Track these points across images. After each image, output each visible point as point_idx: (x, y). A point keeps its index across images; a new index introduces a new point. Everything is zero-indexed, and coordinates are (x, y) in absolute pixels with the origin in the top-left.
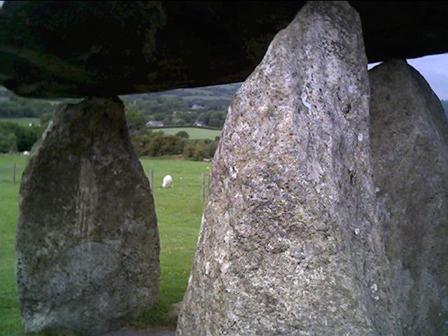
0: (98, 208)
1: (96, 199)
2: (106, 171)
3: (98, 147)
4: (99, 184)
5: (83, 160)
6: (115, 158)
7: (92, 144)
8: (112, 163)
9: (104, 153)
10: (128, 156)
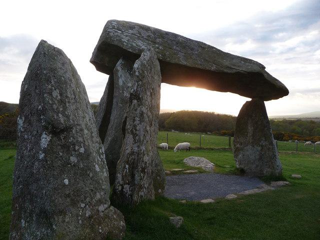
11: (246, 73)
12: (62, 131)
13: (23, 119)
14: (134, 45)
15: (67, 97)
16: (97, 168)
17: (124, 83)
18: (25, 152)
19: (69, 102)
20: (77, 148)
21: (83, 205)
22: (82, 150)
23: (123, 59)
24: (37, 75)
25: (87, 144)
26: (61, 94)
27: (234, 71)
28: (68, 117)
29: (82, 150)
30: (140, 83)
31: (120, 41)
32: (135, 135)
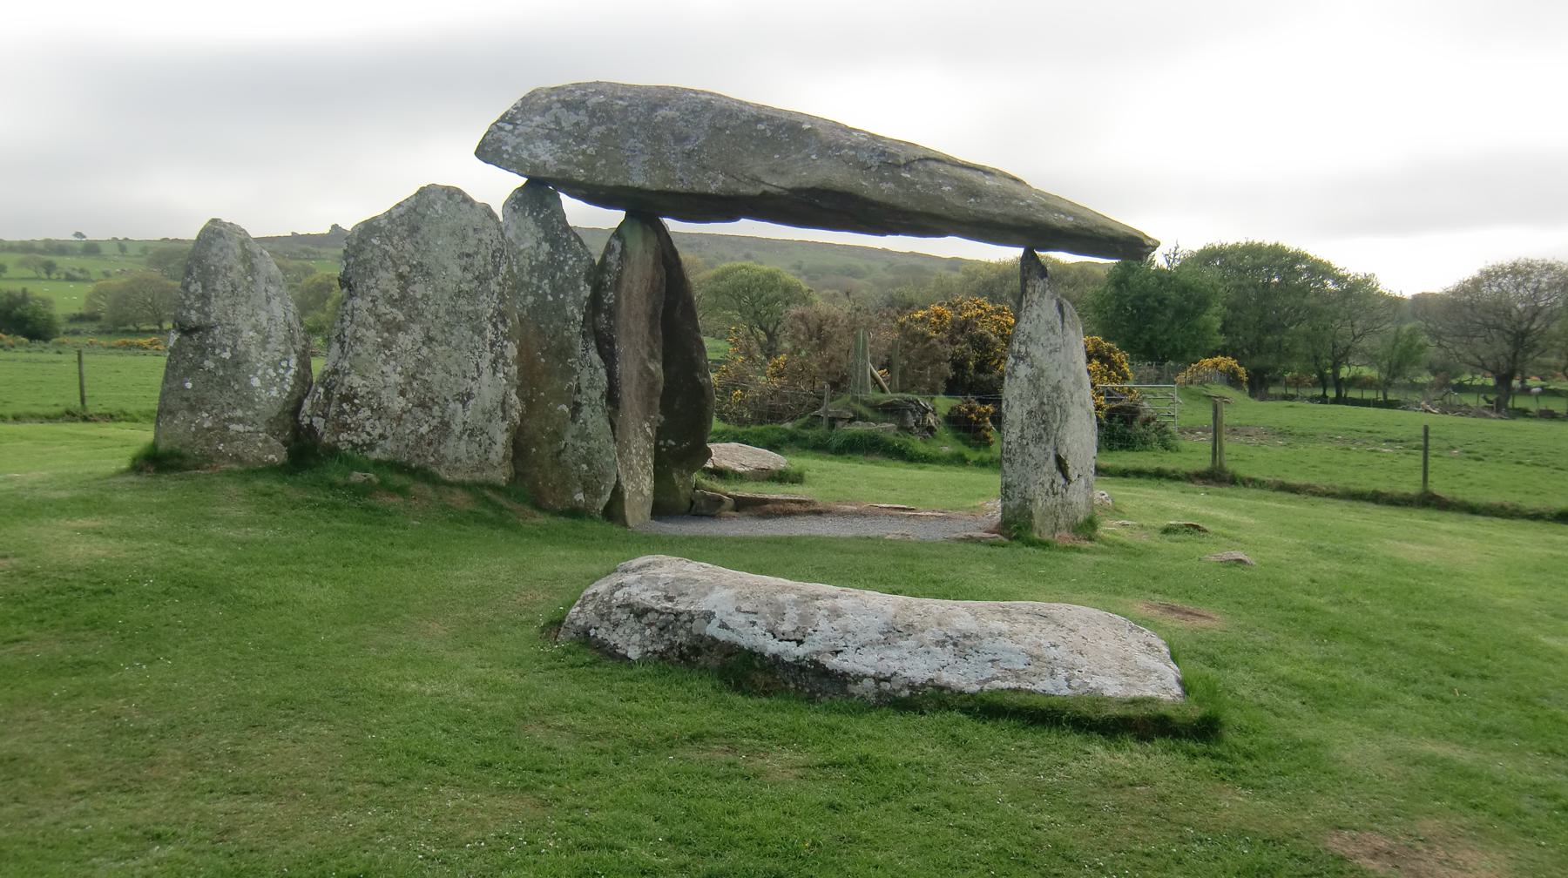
11: (786, 193)
12: (196, 329)
14: (525, 155)
15: (214, 290)
16: (256, 382)
19: (216, 296)
20: (217, 351)
21: (205, 415)
22: (227, 355)
25: (241, 348)
26: (204, 287)
28: (207, 315)
29: (227, 355)
30: (352, 260)
32: (342, 344)
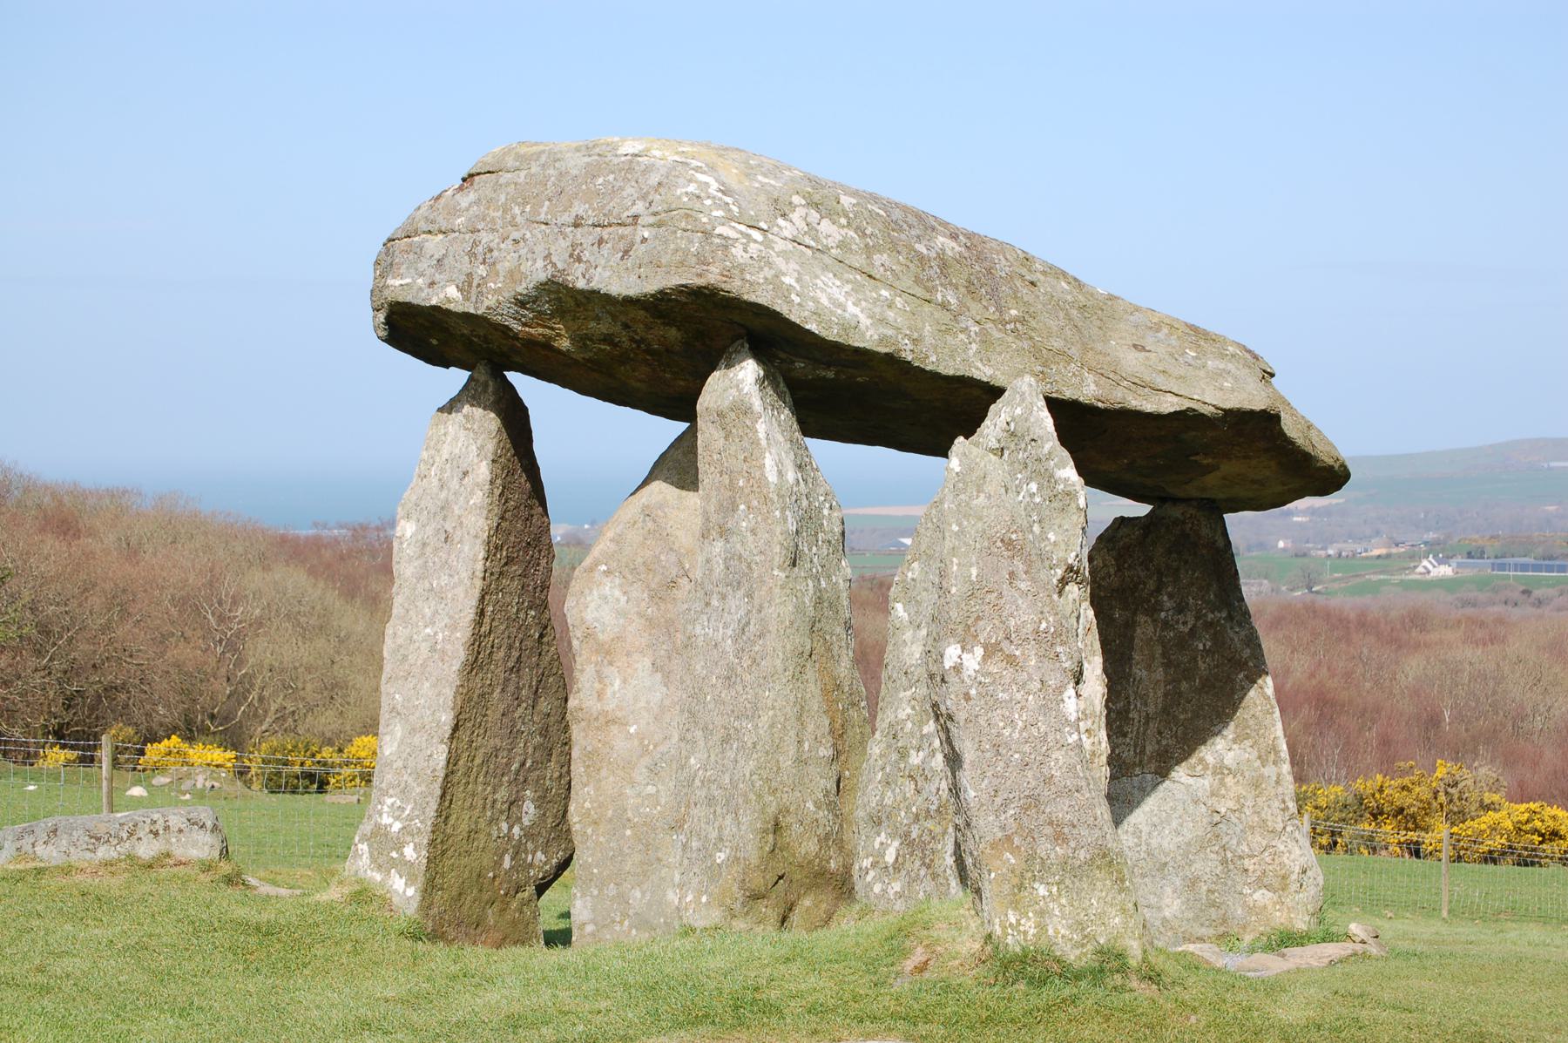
0: (1165, 710)
1: (1160, 694)
2: (1183, 643)
3: (1171, 596)
4: (1168, 665)
5: (1141, 618)
6: (1197, 618)
7: (1158, 590)
8: (1194, 626)
9: (1180, 609)
10: (1224, 615)
13: (979, 651)
14: (825, 301)
17: (780, 473)
18: (1007, 732)
23: (760, 354)
24: (1009, 544)
27: (1168, 405)
31: (775, 282)
